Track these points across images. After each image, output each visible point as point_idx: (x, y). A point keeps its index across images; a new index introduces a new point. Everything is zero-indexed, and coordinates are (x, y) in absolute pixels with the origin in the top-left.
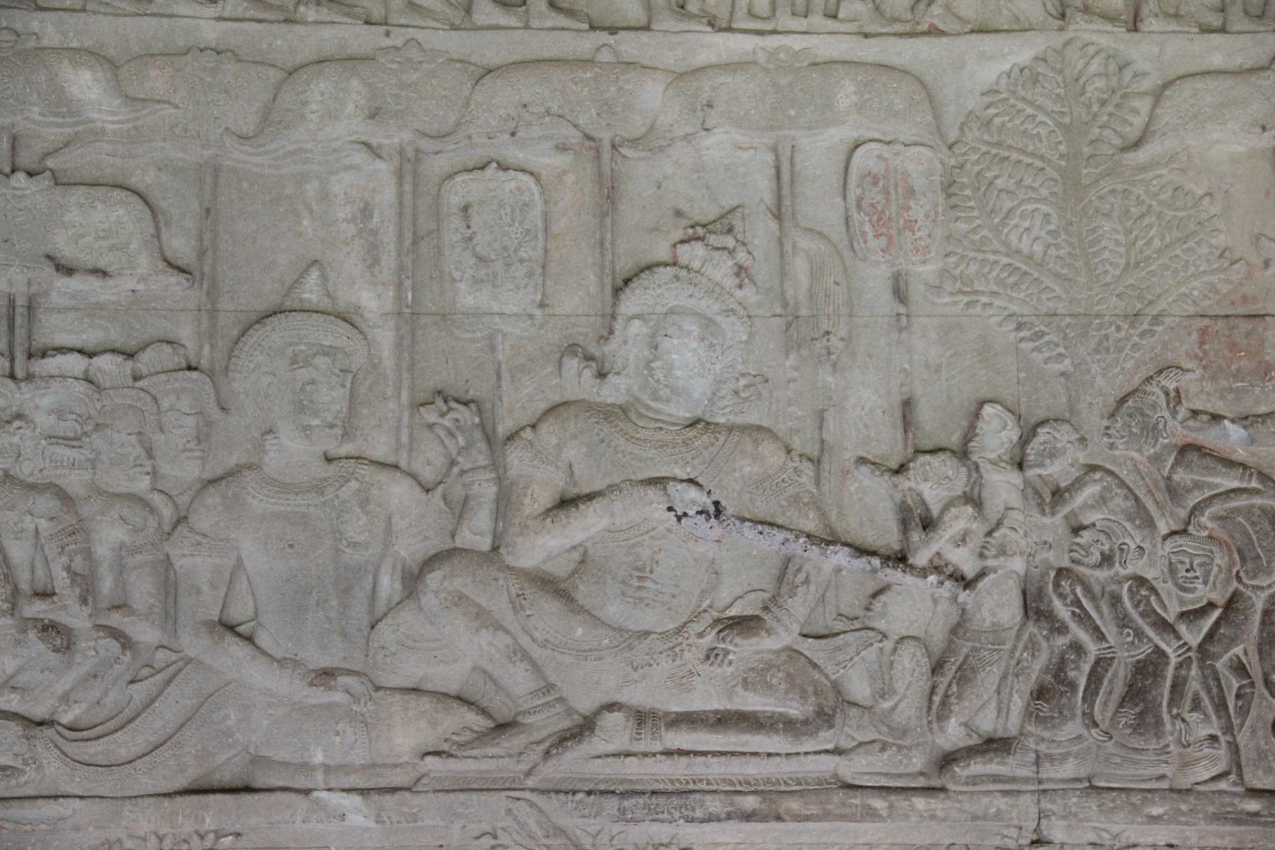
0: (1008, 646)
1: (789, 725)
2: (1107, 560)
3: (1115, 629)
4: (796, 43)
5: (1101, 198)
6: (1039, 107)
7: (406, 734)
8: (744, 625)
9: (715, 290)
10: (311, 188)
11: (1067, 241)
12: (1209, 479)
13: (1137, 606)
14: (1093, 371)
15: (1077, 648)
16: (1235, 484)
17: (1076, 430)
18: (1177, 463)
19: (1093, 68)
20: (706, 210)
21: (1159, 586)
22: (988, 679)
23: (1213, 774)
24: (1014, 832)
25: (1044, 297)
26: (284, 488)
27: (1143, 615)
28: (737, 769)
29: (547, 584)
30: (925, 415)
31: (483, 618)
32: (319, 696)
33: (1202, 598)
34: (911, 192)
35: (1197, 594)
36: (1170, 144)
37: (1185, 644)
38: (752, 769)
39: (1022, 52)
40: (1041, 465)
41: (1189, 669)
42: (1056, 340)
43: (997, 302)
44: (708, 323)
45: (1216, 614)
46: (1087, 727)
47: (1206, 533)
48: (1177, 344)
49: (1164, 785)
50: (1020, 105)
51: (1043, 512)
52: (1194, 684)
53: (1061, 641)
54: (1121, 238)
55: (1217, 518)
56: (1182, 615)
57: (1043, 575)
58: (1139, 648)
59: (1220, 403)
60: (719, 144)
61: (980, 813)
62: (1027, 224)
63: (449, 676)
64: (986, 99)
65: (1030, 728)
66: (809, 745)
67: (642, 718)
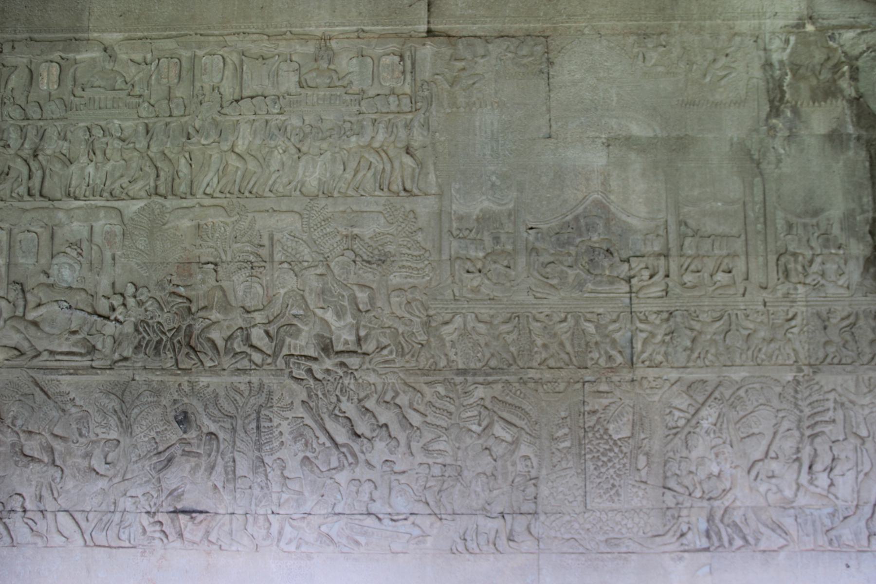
1: (81, 354)
2: (152, 318)
8: (74, 333)
15: (144, 338)
20: (73, 240)
22: (125, 344)
28: (70, 364)
29: (35, 324)
31: (19, 331)
34: (116, 235)
36: (173, 224)
38: (73, 364)
39: (141, 204)
44: (70, 265)
52: (169, 346)
53: (140, 336)
60: (75, 225)
63: (12, 343)
66: (85, 359)
67: (52, 353)
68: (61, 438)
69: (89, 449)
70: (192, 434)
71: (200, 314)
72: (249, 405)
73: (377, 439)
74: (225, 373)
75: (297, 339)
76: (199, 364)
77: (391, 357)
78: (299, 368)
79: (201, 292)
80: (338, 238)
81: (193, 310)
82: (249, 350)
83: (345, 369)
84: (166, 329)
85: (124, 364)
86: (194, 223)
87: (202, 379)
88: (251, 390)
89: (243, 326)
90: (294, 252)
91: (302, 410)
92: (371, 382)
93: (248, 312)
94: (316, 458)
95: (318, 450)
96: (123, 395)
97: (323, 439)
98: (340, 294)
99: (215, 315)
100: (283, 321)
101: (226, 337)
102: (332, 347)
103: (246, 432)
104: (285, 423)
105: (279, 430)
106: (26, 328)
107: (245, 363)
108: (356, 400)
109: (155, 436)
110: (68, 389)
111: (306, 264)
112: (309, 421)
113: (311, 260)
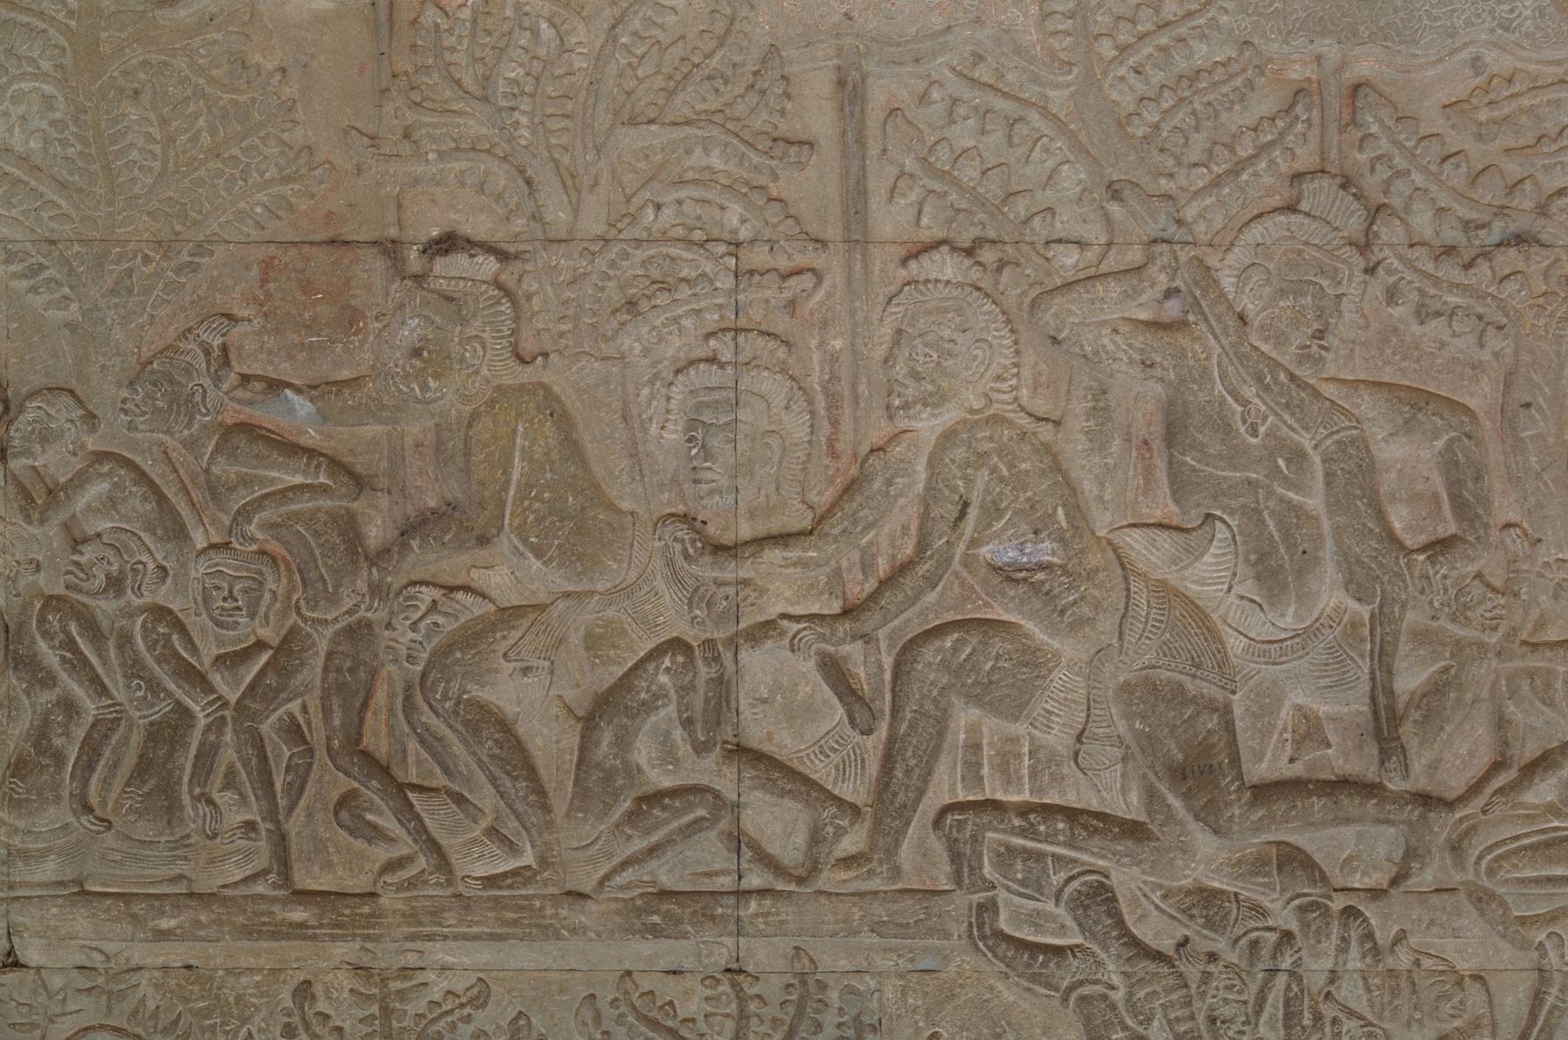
2: (115, 584)
3: (121, 681)
5: (126, 73)
11: (77, 136)
12: (261, 472)
13: (151, 648)
14: (109, 321)
15: (69, 707)
16: (298, 479)
21: (189, 621)
23: (248, 873)
25: (45, 215)
33: (247, 636)
35: (240, 632)
37: (219, 698)
41: (220, 732)
42: (59, 276)
45: (265, 657)
46: (75, 814)
47: (254, 547)
48: (229, 282)
49: (181, 889)
51: (28, 519)
52: (228, 755)
54: (155, 131)
56: (219, 660)
57: (25, 607)
58: (153, 706)
62: (22, 109)
71: (424, 560)
74: (588, 915)
75: (1017, 711)
76: (422, 862)
79: (416, 429)
80: (1264, 104)
81: (376, 532)
82: (725, 780)
83: (1314, 892)
87: (440, 953)
88: (743, 1016)
89: (692, 635)
90: (992, 189)
92: (1463, 966)
93: (719, 549)
99: (505, 574)
100: (932, 607)
102: (1235, 760)
107: (704, 859)
111: (1068, 259)
113: (1095, 233)
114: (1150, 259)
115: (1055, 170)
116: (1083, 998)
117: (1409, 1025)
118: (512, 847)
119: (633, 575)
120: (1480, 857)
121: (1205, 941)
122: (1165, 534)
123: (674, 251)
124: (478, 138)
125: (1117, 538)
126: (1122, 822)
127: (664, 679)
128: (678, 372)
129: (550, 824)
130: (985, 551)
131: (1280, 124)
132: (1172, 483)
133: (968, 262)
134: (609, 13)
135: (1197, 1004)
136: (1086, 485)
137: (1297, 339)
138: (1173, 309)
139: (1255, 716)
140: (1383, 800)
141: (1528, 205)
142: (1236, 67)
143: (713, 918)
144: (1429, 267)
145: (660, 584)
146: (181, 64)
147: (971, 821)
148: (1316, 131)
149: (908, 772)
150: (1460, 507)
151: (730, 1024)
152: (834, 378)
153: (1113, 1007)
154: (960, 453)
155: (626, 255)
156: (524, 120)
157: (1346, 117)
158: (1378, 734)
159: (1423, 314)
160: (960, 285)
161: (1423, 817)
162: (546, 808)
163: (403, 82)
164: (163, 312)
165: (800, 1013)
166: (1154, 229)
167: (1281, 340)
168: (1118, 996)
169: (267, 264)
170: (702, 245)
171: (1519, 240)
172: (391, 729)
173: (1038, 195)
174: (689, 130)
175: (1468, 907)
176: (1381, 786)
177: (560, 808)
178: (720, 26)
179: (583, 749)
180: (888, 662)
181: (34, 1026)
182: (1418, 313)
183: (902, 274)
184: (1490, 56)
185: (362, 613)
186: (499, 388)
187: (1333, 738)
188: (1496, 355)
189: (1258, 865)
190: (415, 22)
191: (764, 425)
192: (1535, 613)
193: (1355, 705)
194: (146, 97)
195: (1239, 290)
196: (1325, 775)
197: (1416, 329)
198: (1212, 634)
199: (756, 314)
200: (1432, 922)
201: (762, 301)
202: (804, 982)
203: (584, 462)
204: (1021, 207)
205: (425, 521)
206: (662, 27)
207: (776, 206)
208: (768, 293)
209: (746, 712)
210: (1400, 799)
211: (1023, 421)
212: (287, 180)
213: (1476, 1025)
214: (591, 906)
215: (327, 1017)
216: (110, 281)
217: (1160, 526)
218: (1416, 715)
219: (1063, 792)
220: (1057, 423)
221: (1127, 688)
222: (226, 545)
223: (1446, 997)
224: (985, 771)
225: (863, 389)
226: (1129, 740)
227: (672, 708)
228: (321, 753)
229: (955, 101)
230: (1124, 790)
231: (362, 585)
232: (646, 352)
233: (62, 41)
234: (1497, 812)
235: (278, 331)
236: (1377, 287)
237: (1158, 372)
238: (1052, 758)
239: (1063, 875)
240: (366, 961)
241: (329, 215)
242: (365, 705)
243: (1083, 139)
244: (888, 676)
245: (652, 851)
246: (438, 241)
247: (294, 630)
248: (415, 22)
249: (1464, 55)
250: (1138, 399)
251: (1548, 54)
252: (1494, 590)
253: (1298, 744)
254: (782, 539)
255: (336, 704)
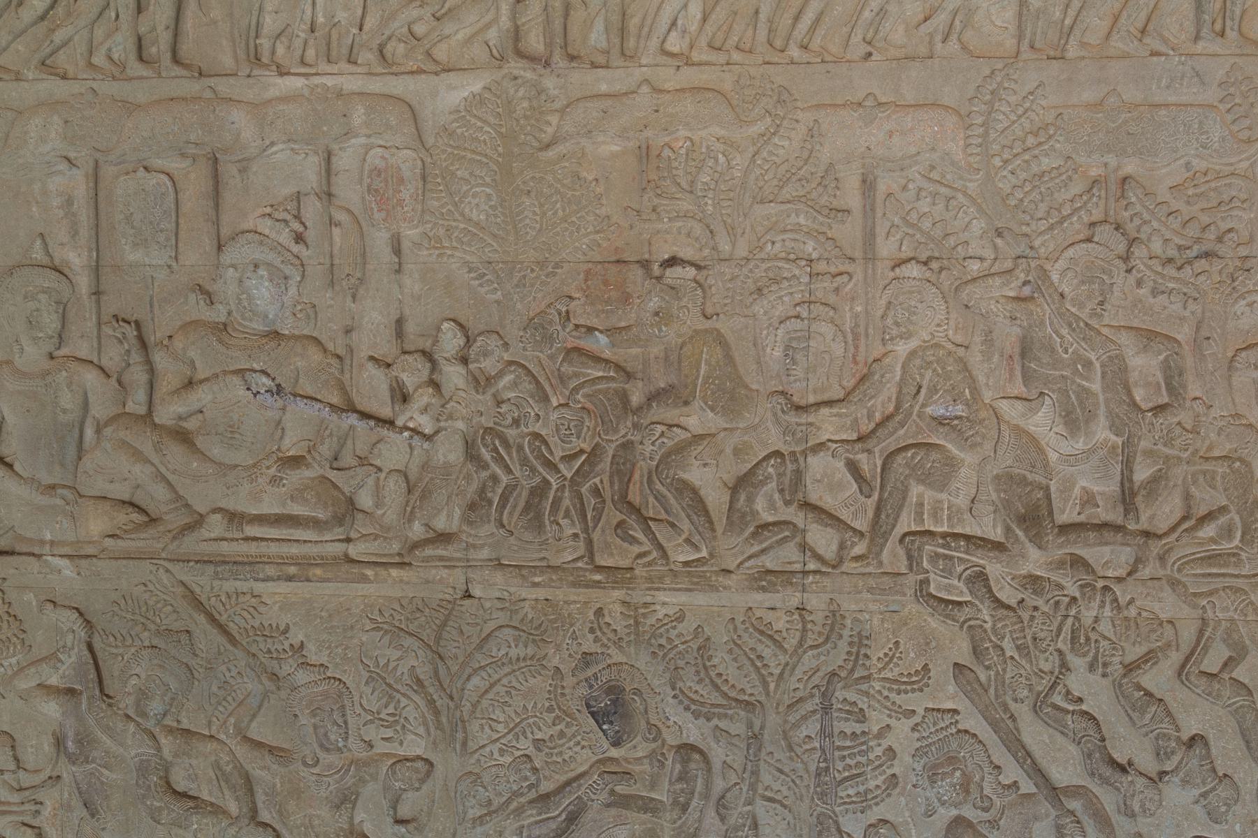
0: (454, 477)
1: (316, 523)
2: (516, 422)
4: (329, 81)
6: (485, 122)
7: (96, 524)
8: (296, 461)
9: (279, 248)
10: (37, 187)
13: (532, 452)
15: (495, 479)
16: (600, 374)
17: (501, 338)
18: (563, 360)
19: (521, 94)
21: (550, 440)
24: (451, 591)
26: (24, 375)
27: (536, 458)
28: (286, 550)
30: (410, 328)
31: (138, 455)
32: (43, 500)
34: (401, 181)
38: (295, 550)
39: (474, 85)
40: (477, 361)
41: (563, 492)
43: (457, 254)
45: (584, 457)
50: (473, 121)
51: (477, 392)
52: (566, 502)
55: (586, 396)
56: (563, 458)
57: (476, 432)
59: (595, 320)
61: (431, 578)
64: (452, 117)
65: (465, 528)
67: (234, 518)
68: (271, 750)
69: (349, 781)
70: (637, 749)
71: (659, 412)
72: (798, 673)
73: (1176, 780)
74: (731, 581)
75: (942, 487)
76: (655, 554)
77: (1226, 546)
78: (947, 572)
79: (656, 350)
81: (636, 399)
82: (799, 519)
83: (1088, 578)
84: (559, 453)
85: (440, 552)
86: (632, 144)
87: (662, 596)
88: (804, 630)
89: (784, 449)
90: (938, 232)
91: (952, 688)
92: (1163, 616)
93: (799, 408)
94: (994, 824)
95: (998, 802)
96: (438, 638)
97: (1013, 772)
98: (1077, 358)
99: (696, 419)
100: (902, 436)
101: (730, 478)
102: (1051, 513)
103: (791, 749)
104: (903, 727)
105: (885, 743)
106: (157, 448)
107: (786, 556)
108: (1116, 669)
109: (531, 751)
110: (285, 619)
111: (975, 266)
112: (973, 721)
114: (1016, 266)
115: (969, 222)
116: (970, 627)
117: (1134, 644)
118: (697, 548)
119: (757, 420)
120: (1174, 563)
121: (1033, 600)
122: (1019, 402)
123: (780, 264)
124: (688, 211)
125: (995, 404)
126: (993, 542)
127: (770, 470)
128: (781, 322)
129: (715, 538)
130: (929, 410)
131: (1085, 198)
132: (1023, 377)
133: (925, 268)
134: (752, 149)
135: (1027, 631)
136: (980, 378)
137: (1090, 305)
138: (1027, 291)
139: (1062, 492)
140: (1126, 534)
141: (1212, 237)
142: (1063, 170)
143: (791, 584)
144: (1159, 269)
145: (769, 424)
146: (550, 178)
147: (918, 539)
148: (1103, 201)
149: (888, 516)
150: (1171, 389)
151: (798, 634)
152: (857, 325)
153: (985, 631)
154: (918, 362)
155: (757, 266)
156: (710, 202)
157: (1119, 194)
158: (1124, 501)
159: (1155, 292)
160: (920, 280)
161: (1146, 542)
162: (713, 530)
163: (652, 185)
164: (539, 295)
165: (832, 630)
166: (1018, 251)
167: (1081, 306)
168: (988, 626)
169: (588, 272)
170: (794, 261)
171: (1207, 255)
172: (641, 491)
173: (961, 235)
174: (789, 205)
175: (1167, 588)
176: (1124, 527)
177: (720, 530)
178: (805, 154)
179: (731, 502)
180: (879, 463)
181: (477, 624)
182: (1153, 292)
183: (892, 274)
184: (1195, 162)
185: (629, 437)
186: (695, 331)
187: (1100, 503)
188: (1192, 313)
189: (1061, 564)
190: (659, 155)
191: (822, 348)
192: (1207, 443)
193: (1113, 487)
194: (533, 194)
195: (1061, 281)
196: (1095, 522)
197: (1152, 300)
198: (1041, 451)
199: (820, 294)
200: (1148, 594)
201: (823, 287)
202: (834, 615)
203: (735, 366)
204: (952, 241)
205: (659, 394)
206: (777, 155)
207: (831, 242)
208: (826, 284)
209: (809, 487)
210: (1134, 534)
211: (950, 346)
212: (598, 232)
213: (1169, 645)
214: (733, 576)
215: (609, 624)
216: (515, 281)
217: (1017, 398)
218: (1143, 492)
219: (963, 527)
220: (967, 347)
221: (997, 477)
222: (567, 405)
223: (1154, 631)
224: (925, 516)
225: (871, 331)
226: (997, 502)
227: (774, 484)
228: (609, 502)
229: (920, 189)
230: (994, 527)
231: (629, 424)
232: (766, 313)
233: (495, 168)
234: (1184, 541)
235: (592, 304)
236: (1131, 280)
237: (1018, 322)
238: (959, 511)
239: (963, 567)
240: (628, 599)
241: (617, 249)
242: (629, 480)
243: (984, 206)
244: (879, 470)
245: (763, 551)
246: (667, 261)
247: (597, 445)
248: (659, 155)
249: (1182, 161)
250: (1009, 335)
251: (1225, 160)
252: (1187, 431)
253: (1083, 506)
254: (830, 403)
255: (616, 479)
